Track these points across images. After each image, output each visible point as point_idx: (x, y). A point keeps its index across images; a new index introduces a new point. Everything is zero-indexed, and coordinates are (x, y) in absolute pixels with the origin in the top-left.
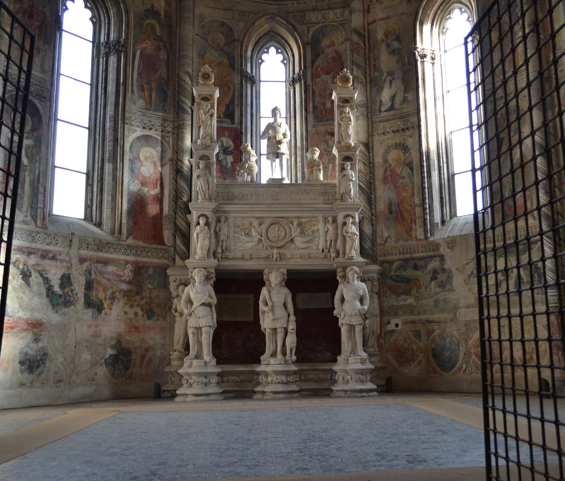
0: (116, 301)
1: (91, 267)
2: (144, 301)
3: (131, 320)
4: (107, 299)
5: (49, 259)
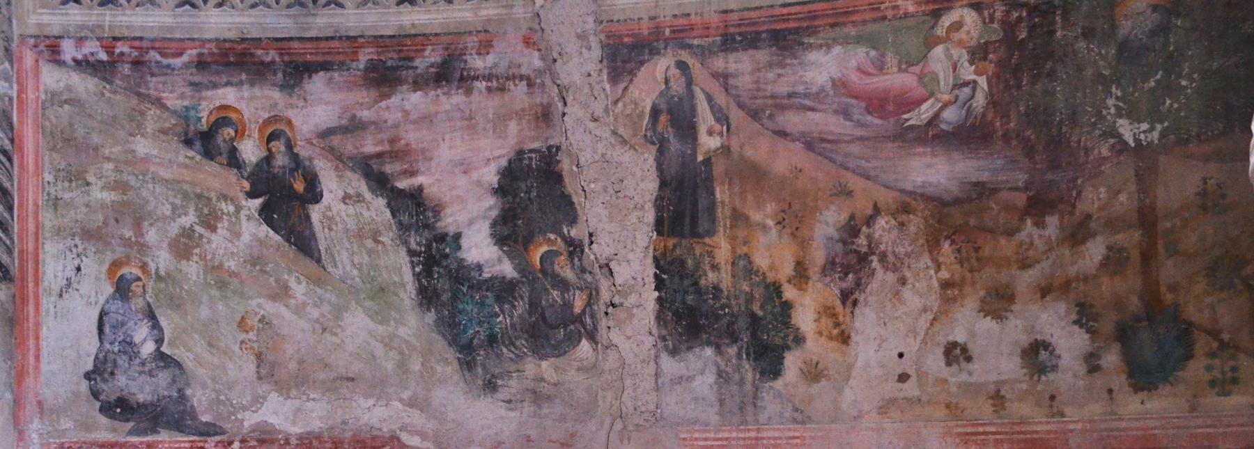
0: (882, 278)
1: (690, 83)
2: (1095, 251)
3: (998, 398)
4: (814, 272)
5: (417, 85)
